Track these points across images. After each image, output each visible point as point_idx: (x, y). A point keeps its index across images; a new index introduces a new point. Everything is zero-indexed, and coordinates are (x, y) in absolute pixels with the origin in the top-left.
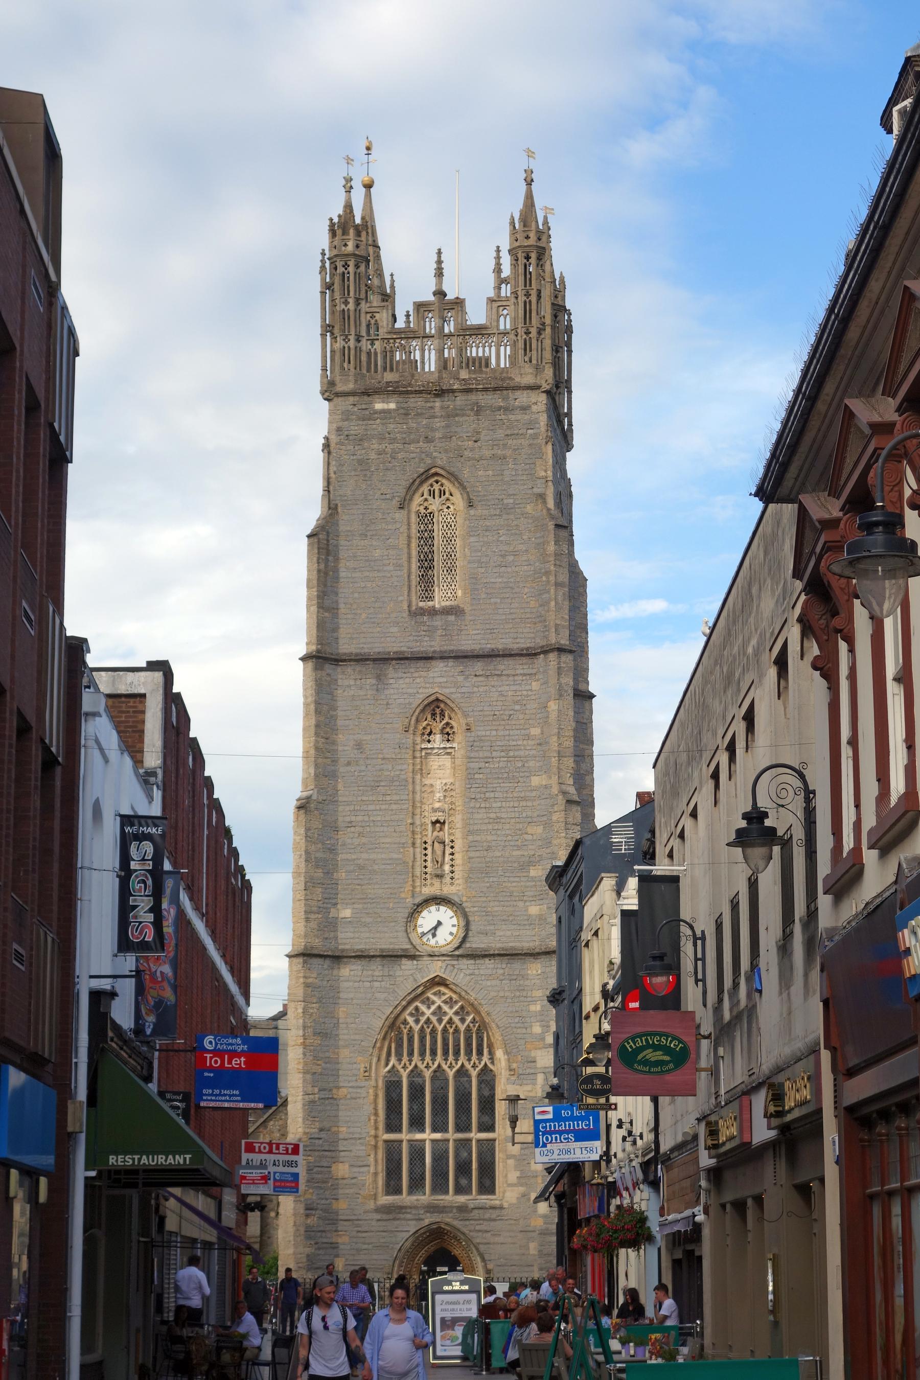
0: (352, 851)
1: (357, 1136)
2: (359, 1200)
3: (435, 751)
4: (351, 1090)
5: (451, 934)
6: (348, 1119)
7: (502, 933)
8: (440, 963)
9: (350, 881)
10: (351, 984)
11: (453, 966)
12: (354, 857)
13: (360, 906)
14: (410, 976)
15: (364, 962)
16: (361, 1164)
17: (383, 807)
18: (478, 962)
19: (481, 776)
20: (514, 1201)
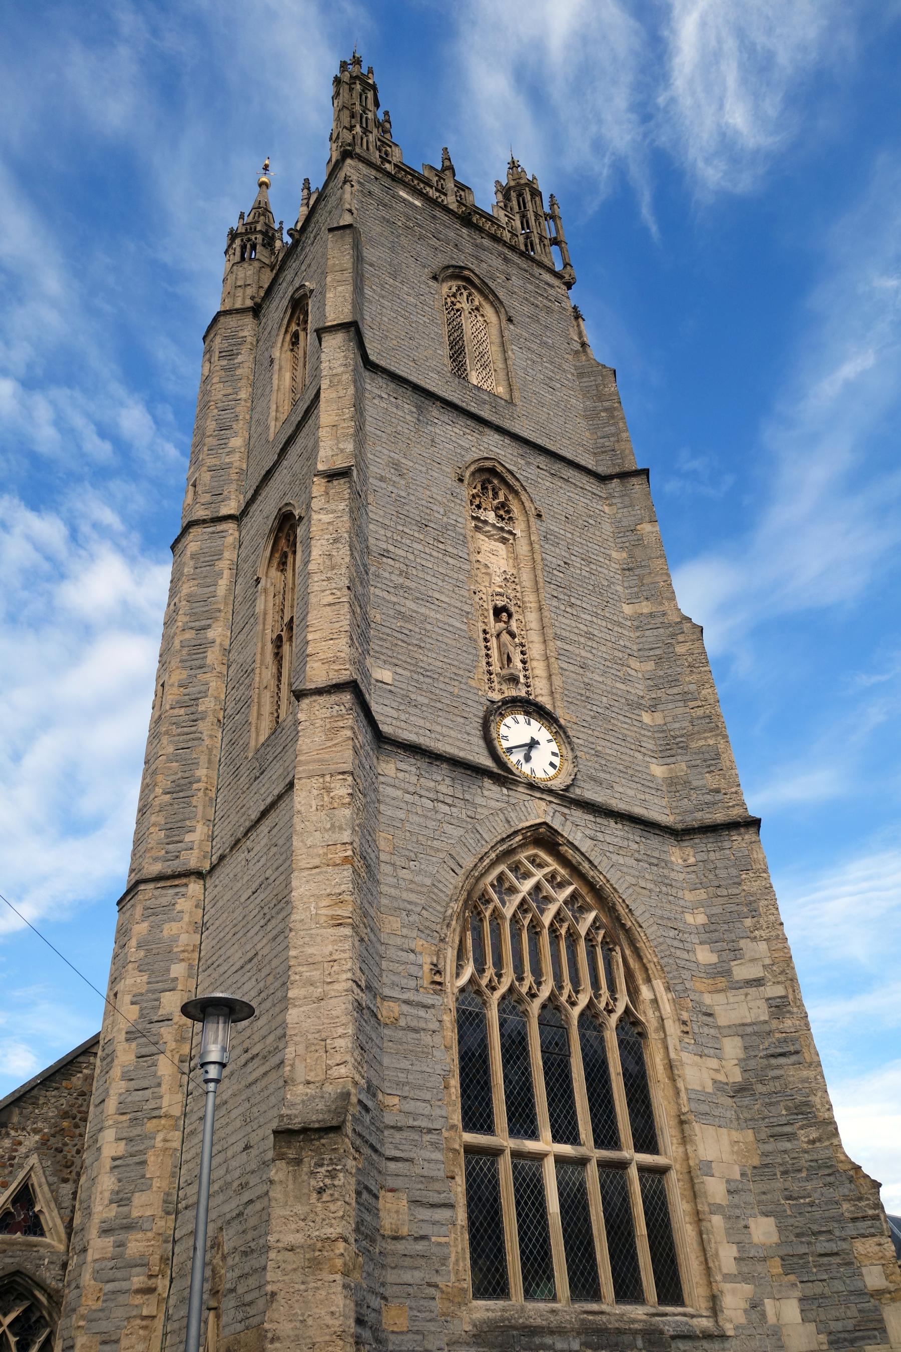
0: (392, 590)
1: (423, 1123)
2: (438, 1305)
3: (488, 528)
4: (406, 1008)
5: (552, 765)
6: (402, 1076)
7: (621, 790)
8: (543, 804)
9: (388, 631)
10: (399, 793)
11: (564, 815)
12: (394, 599)
13: (407, 673)
14: (501, 813)
15: (423, 764)
16: (435, 1198)
17: (435, 554)
18: (598, 820)
19: (561, 575)
20: (742, 1319)
